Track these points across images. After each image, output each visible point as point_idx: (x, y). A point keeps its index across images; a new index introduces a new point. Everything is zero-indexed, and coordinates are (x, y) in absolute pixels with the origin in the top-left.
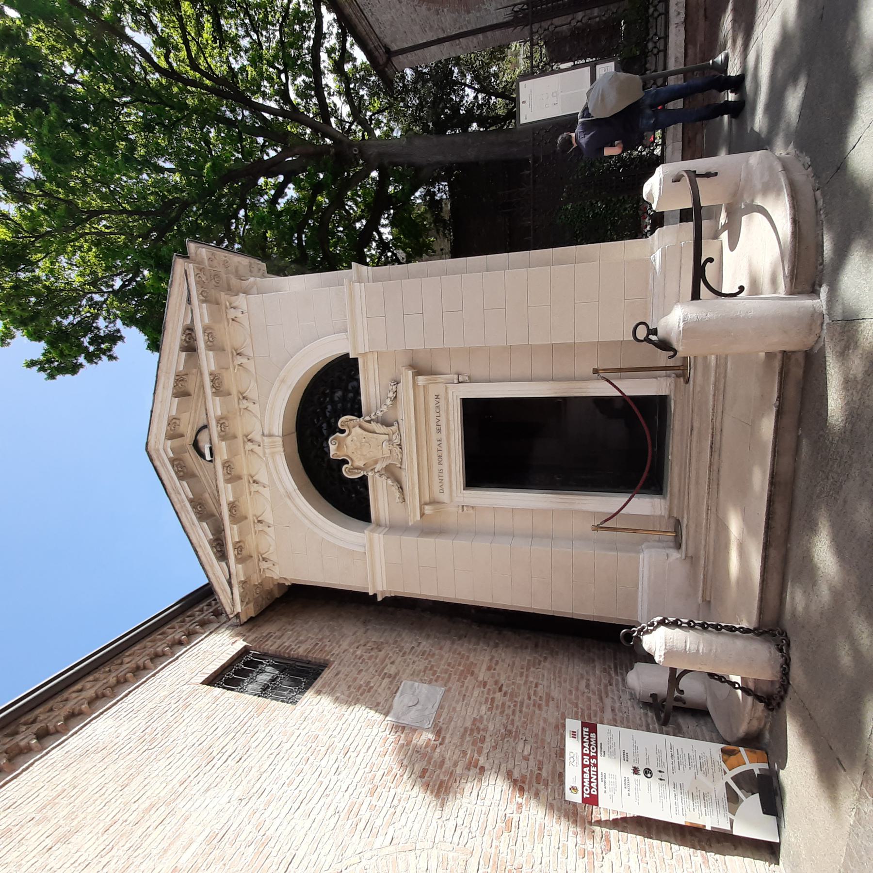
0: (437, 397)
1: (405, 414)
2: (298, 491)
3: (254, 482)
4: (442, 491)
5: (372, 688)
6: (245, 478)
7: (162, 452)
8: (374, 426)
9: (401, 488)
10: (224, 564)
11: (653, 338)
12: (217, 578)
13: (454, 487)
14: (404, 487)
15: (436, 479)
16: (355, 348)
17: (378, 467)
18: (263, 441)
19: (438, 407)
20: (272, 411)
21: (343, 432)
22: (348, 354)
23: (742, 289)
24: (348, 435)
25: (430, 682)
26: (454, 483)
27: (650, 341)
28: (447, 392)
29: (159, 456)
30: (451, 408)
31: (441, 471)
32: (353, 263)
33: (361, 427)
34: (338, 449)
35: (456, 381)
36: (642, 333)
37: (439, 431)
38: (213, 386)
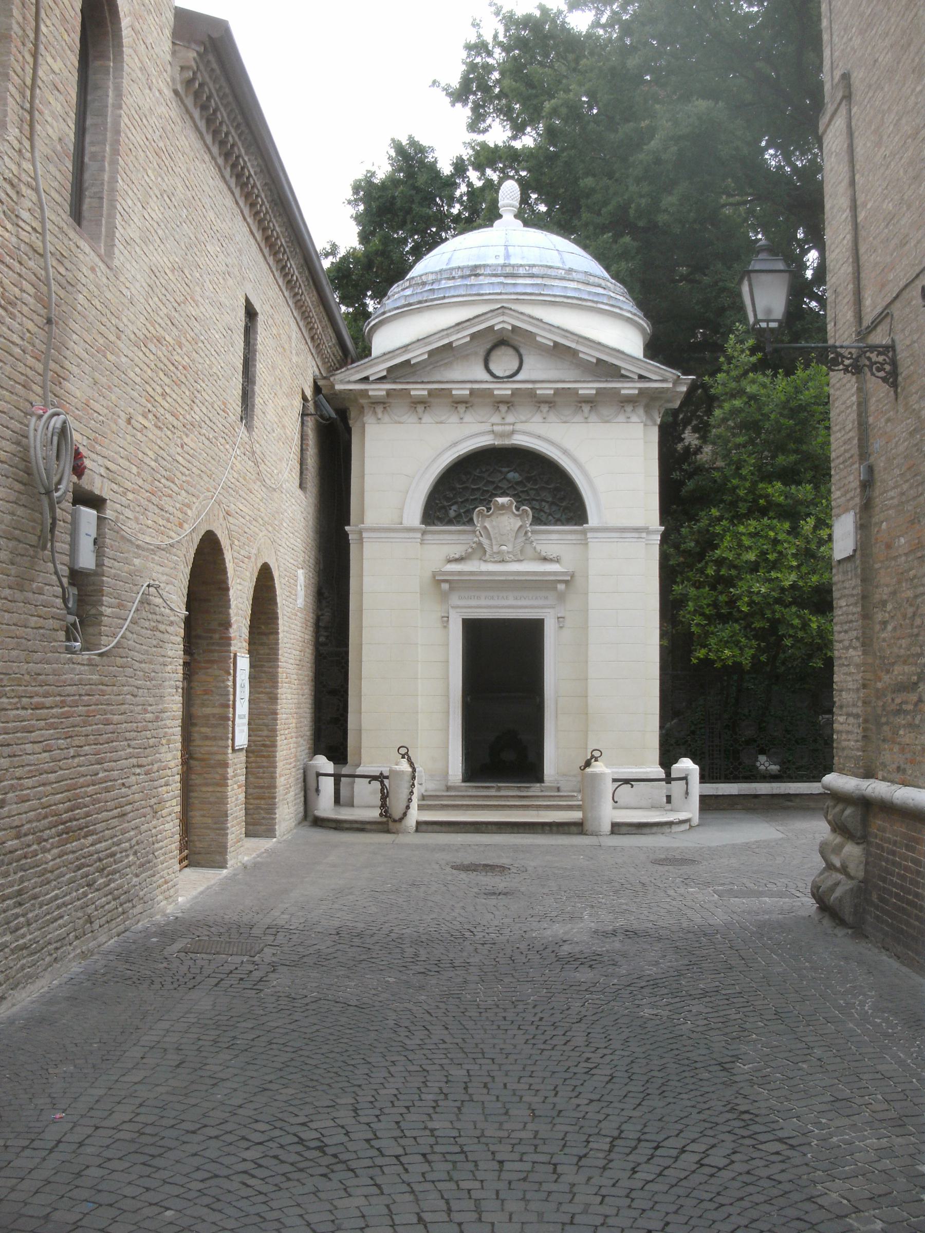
0: (546, 598)
2: (457, 455)
4: (460, 598)
9: (460, 560)
10: (384, 373)
13: (465, 610)
20: (536, 433)
21: (518, 509)
26: (469, 610)
30: (536, 610)
31: (479, 598)
32: (663, 528)
33: (521, 527)
34: (503, 507)
35: (559, 615)
36: (597, 754)
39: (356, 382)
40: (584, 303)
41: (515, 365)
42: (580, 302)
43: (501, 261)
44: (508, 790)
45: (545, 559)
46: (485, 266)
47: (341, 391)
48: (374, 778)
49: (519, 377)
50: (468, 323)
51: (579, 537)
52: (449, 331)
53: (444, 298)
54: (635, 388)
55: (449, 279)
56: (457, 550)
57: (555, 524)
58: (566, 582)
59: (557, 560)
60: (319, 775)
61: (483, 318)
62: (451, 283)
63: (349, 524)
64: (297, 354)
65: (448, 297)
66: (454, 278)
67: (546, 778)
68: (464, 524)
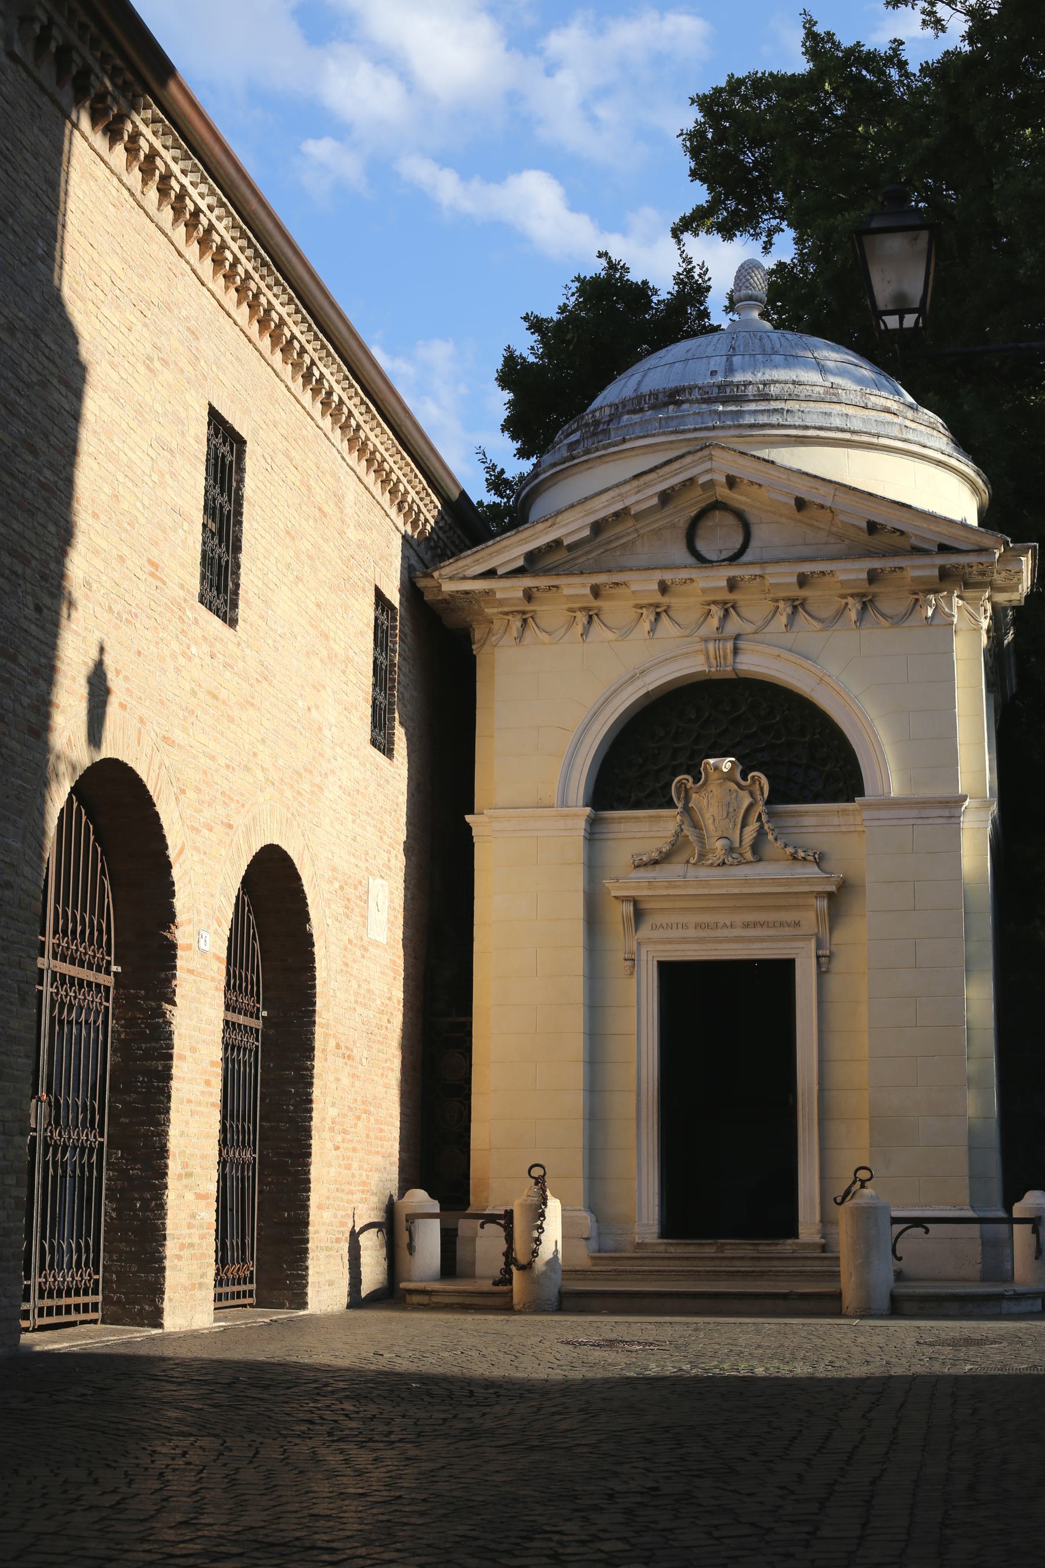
1: (773, 872)
3: (658, 614)
4: (655, 927)
5: (382, 838)
6: (665, 600)
7: (707, 465)
9: (656, 862)
10: (520, 563)
11: (858, 1183)
12: (498, 552)
14: (658, 867)
15: (674, 918)
16: (869, 806)
18: (725, 639)
19: (782, 924)
22: (862, 794)
23: (900, 1259)
25: (388, 920)
26: (669, 947)
27: (854, 1183)
28: (805, 937)
29: (702, 461)
30: (781, 945)
31: (685, 926)
33: (751, 806)
35: (820, 953)
36: (863, 1175)
37: (746, 925)
38: (813, 573)
39: (475, 578)
40: (855, 438)
41: (737, 542)
42: (847, 436)
43: (720, 378)
44: (738, 1251)
45: (795, 858)
46: (691, 389)
47: (454, 595)
48: (492, 1219)
49: (745, 558)
50: (652, 476)
52: (623, 489)
53: (624, 441)
54: (933, 566)
55: (634, 412)
57: (815, 800)
58: (830, 895)
60: (412, 1218)
61: (676, 465)
62: (636, 417)
63: (471, 812)
64: (359, 525)
65: (631, 439)
66: (641, 410)
67: (802, 1230)
68: (661, 806)
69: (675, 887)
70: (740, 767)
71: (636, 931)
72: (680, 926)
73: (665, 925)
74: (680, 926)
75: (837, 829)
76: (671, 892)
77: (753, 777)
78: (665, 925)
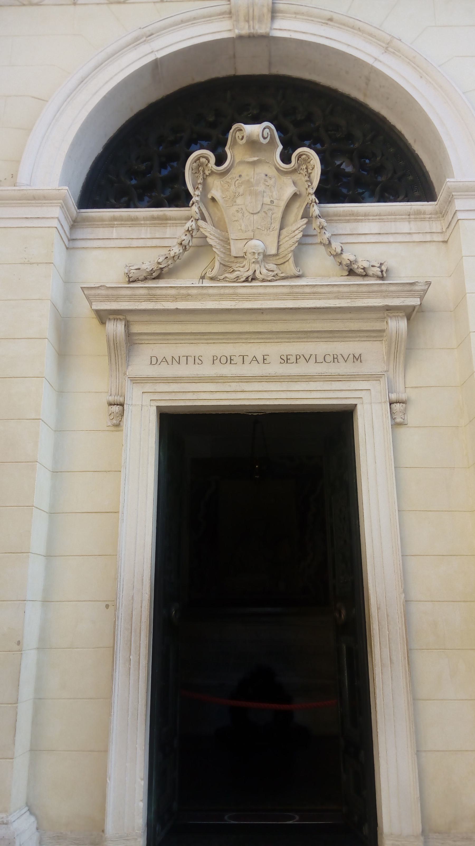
0: (357, 358)
8: (296, 225)
17: (207, 228)
19: (335, 358)
24: (278, 169)
31: (198, 360)
33: (295, 196)
35: (394, 397)
37: (286, 360)
45: (351, 273)
51: (426, 226)
56: (148, 260)
58: (410, 314)
59: (382, 278)
69: (187, 297)
70: (280, 147)
71: (128, 365)
72: (191, 360)
73: (169, 360)
74: (191, 360)
75: (407, 238)
76: (182, 305)
77: (300, 156)
78: (169, 360)
